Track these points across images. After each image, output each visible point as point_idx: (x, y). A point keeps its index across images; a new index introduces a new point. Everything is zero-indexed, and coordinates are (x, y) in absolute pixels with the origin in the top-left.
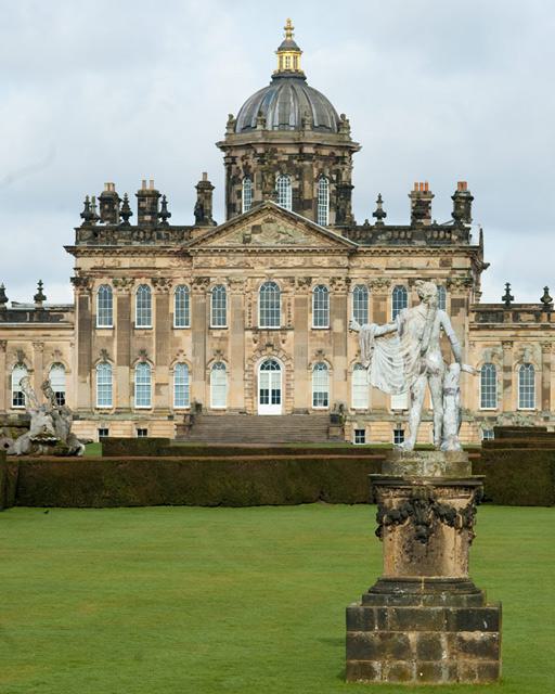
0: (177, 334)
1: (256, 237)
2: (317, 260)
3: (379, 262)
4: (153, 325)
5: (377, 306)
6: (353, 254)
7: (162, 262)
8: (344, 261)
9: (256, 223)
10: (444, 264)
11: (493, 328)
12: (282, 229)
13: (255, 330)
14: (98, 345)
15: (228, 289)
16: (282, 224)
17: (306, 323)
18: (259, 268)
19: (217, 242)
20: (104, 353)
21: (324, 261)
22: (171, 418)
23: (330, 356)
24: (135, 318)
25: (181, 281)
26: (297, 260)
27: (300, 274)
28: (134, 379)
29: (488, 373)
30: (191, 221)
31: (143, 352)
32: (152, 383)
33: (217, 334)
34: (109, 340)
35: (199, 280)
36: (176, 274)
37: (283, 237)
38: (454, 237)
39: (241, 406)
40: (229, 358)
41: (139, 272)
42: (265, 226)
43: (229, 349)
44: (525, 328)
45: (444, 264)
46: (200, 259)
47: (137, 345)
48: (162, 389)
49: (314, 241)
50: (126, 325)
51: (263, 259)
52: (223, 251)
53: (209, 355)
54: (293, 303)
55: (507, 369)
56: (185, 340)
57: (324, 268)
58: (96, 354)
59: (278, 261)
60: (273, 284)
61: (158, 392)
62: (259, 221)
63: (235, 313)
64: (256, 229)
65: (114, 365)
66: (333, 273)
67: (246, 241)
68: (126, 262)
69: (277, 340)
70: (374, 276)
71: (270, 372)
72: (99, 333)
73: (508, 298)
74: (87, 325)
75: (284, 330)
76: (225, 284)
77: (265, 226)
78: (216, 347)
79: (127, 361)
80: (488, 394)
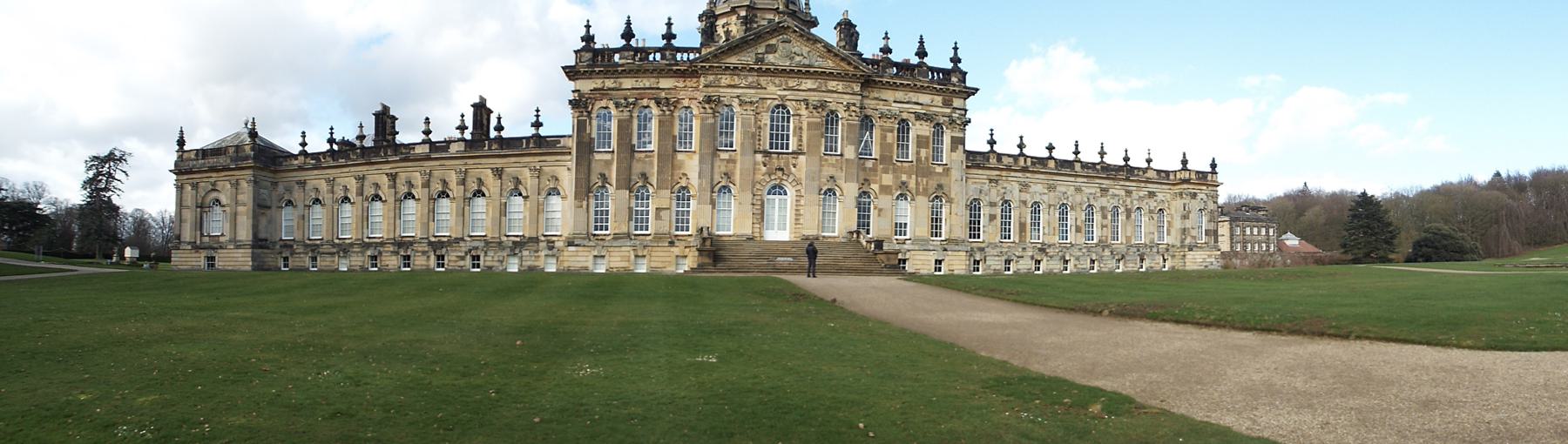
0: (680, 157)
1: (770, 58)
2: (832, 84)
3: (889, 95)
4: (653, 147)
5: (884, 138)
6: (868, 83)
7: (666, 83)
8: (857, 88)
9: (773, 41)
10: (947, 104)
11: (984, 168)
12: (796, 49)
13: (766, 153)
14: (596, 169)
15: (737, 109)
16: (798, 46)
17: (819, 147)
18: (771, 88)
19: (733, 60)
20: (604, 177)
21: (840, 86)
22: (672, 244)
23: (841, 182)
24: (635, 141)
25: (686, 103)
26: (809, 84)
27: (814, 98)
28: (633, 204)
29: (974, 207)
30: (696, 41)
31: (644, 176)
32: (652, 209)
33: (724, 156)
34: (608, 163)
35: (709, 100)
36: (681, 95)
37: (798, 59)
38: (954, 79)
39: (748, 232)
40: (738, 182)
41: (641, 93)
42: (781, 46)
43: (738, 172)
44: (1009, 169)
45: (947, 104)
46: (711, 78)
47: (637, 168)
48: (662, 213)
49: (829, 64)
50: (628, 150)
51: (777, 81)
52: (735, 70)
53: (717, 178)
54: (805, 126)
55: (992, 204)
56: (691, 165)
57: (841, 96)
58: (595, 178)
59: (792, 83)
60: (784, 107)
61: (658, 217)
62: (773, 41)
63: (745, 133)
64: (771, 49)
65: (611, 190)
66: (847, 99)
67: (759, 60)
68: (628, 83)
69: (787, 164)
70: (882, 107)
71: (777, 197)
72: (598, 157)
73: (992, 143)
74: (586, 148)
75: (797, 153)
76: (735, 103)
77: (781, 46)
78: (723, 169)
79: (626, 183)
80: (974, 229)
